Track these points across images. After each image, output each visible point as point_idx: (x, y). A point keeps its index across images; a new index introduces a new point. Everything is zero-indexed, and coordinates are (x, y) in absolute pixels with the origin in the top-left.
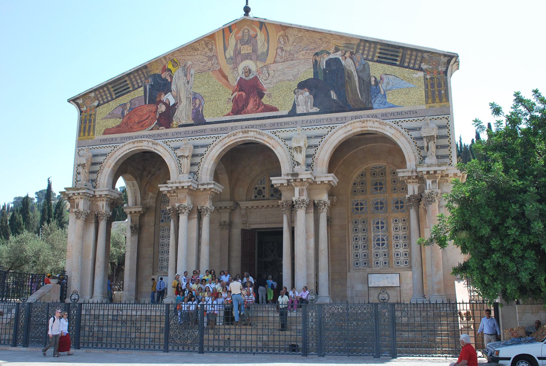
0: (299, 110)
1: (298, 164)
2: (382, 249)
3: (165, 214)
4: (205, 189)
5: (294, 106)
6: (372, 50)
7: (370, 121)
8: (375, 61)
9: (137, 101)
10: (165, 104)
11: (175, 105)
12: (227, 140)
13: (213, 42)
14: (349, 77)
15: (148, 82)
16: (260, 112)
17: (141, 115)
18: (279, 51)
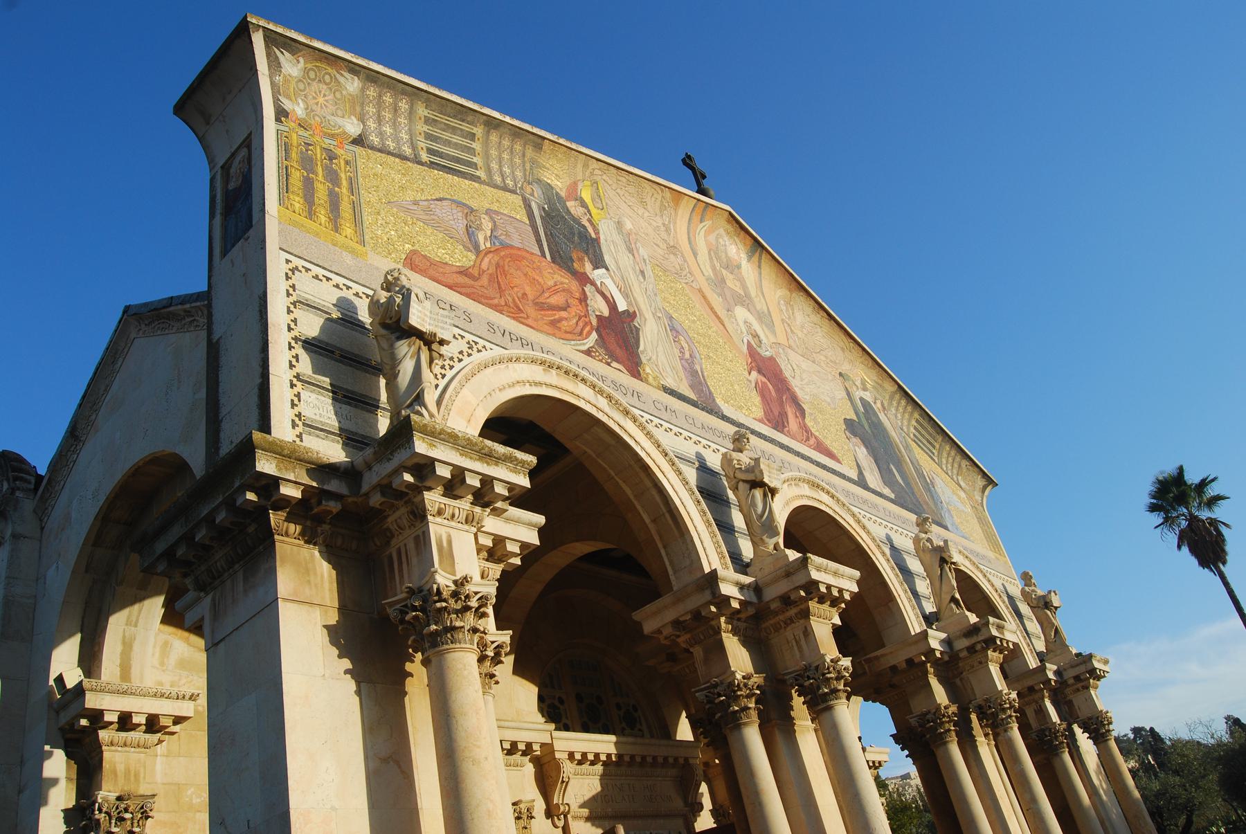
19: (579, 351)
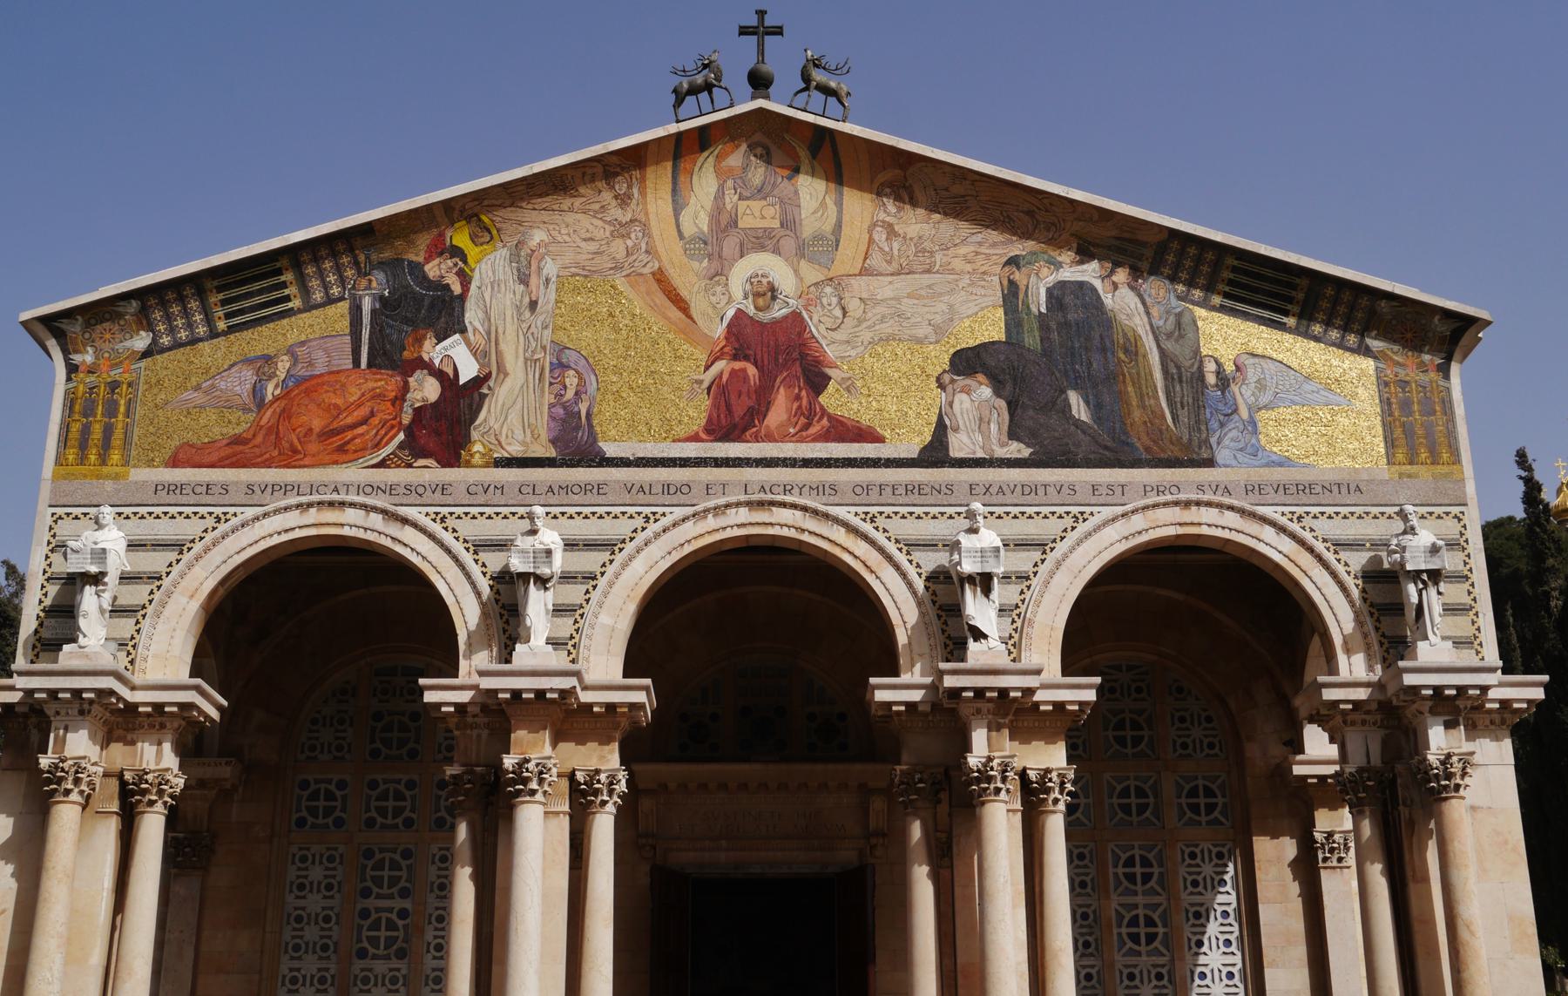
0: (960, 445)
1: (979, 635)
2: (1149, 954)
3: (314, 796)
4: (611, 707)
5: (941, 429)
6: (1205, 269)
7: (1209, 504)
8: (1213, 308)
9: (321, 353)
10: (439, 374)
11: (478, 382)
12: (690, 529)
13: (636, 173)
14: (1126, 351)
15: (369, 287)
16: (814, 440)
17: (336, 406)
18: (880, 235)
19: (368, 467)
